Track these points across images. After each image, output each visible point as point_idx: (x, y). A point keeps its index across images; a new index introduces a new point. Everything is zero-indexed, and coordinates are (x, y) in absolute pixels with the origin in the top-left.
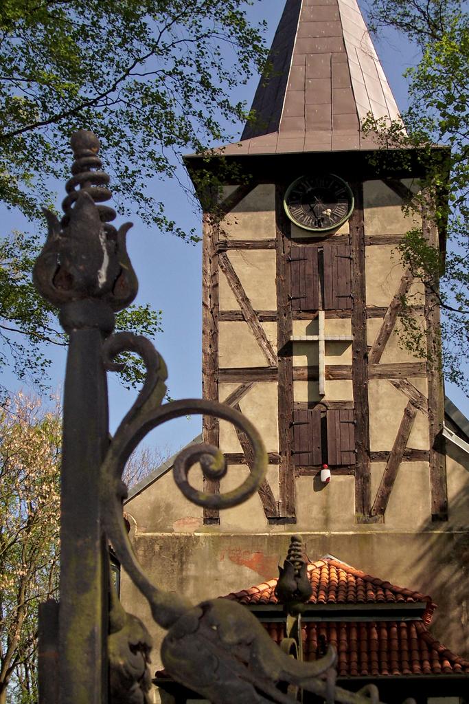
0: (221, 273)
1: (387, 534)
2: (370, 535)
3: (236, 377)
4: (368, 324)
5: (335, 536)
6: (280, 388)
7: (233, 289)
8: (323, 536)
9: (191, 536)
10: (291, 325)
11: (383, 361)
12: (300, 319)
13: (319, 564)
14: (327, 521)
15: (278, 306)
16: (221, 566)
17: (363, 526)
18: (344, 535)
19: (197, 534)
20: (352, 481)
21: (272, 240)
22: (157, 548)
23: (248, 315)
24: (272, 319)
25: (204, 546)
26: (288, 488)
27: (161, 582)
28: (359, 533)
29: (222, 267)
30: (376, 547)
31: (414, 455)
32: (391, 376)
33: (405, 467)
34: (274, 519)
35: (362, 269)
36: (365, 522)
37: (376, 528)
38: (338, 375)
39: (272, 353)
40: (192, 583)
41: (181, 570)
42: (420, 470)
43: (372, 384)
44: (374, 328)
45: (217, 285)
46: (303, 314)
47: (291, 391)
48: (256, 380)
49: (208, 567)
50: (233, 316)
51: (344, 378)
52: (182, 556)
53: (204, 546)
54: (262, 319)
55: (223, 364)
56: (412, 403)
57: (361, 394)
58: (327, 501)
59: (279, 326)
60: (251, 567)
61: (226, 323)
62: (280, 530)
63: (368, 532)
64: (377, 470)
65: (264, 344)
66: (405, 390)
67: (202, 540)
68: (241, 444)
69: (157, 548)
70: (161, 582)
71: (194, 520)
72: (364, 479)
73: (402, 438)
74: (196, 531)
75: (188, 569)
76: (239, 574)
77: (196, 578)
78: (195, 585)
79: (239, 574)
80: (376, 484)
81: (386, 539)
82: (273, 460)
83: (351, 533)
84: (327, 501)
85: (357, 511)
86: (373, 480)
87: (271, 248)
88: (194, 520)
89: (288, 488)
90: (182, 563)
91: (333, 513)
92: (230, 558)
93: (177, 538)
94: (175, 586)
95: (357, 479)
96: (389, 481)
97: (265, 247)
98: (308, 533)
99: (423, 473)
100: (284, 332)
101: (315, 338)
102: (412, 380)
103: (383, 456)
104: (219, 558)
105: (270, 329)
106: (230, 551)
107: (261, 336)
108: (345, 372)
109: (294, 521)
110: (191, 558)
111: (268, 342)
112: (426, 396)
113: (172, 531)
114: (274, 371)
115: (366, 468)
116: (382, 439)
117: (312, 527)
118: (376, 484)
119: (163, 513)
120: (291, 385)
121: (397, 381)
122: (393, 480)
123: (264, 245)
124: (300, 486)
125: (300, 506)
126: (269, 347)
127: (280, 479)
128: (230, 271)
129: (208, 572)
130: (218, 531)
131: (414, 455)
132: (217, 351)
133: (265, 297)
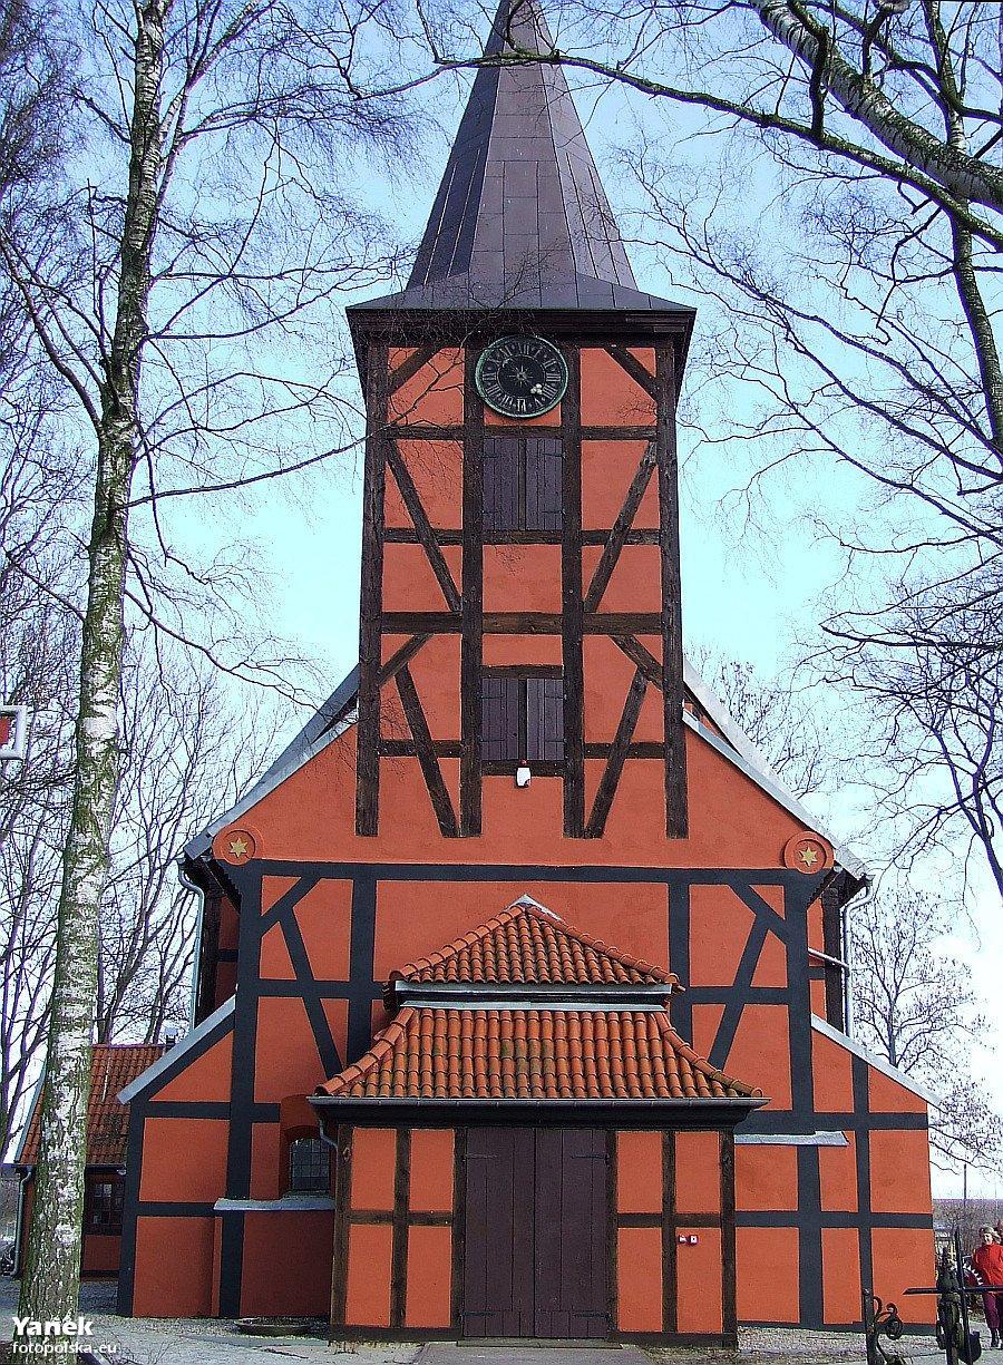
23: (425, 535)
26: (471, 793)
31: (647, 750)
50: (401, 535)
55: (388, 606)
64: (594, 770)
72: (575, 781)
73: (628, 724)
82: (451, 749)
89: (471, 793)
96: (609, 787)
103: (599, 750)
105: (454, 555)
116: (601, 726)
123: (447, 434)
131: (647, 750)
133: (447, 513)
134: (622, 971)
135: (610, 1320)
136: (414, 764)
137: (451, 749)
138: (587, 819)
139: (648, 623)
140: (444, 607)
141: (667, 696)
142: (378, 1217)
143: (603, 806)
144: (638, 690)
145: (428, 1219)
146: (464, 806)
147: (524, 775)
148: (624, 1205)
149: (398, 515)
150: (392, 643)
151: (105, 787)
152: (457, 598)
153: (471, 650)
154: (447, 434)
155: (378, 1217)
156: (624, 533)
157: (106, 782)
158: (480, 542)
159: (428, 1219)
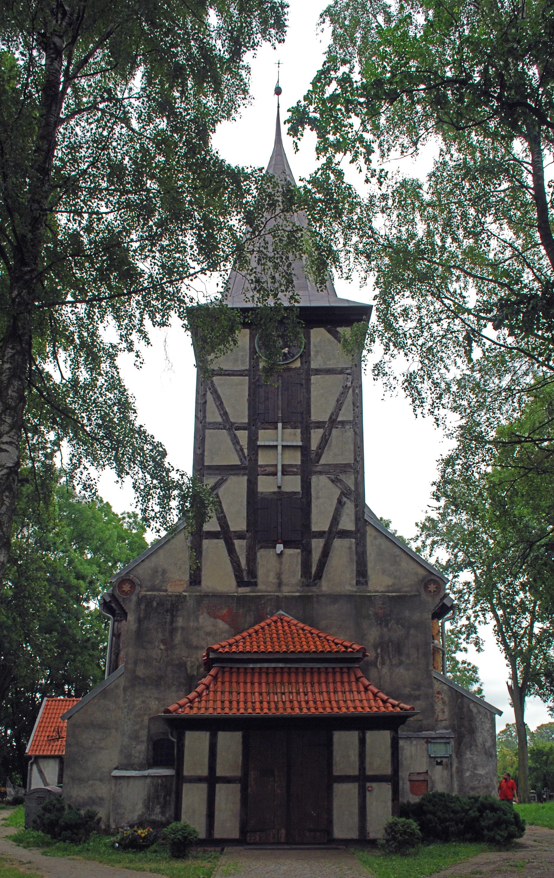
0: (209, 393)
1: (323, 596)
2: (311, 596)
3: (217, 472)
4: (312, 434)
5: (286, 596)
6: (249, 481)
7: (217, 406)
8: (278, 596)
9: (180, 595)
10: (257, 434)
11: (322, 462)
12: (265, 429)
13: (274, 618)
15: (249, 419)
16: (201, 620)
17: (306, 588)
18: (293, 596)
19: (184, 594)
20: (298, 553)
21: (246, 370)
22: (155, 604)
24: (244, 429)
25: (190, 603)
27: (157, 632)
28: (303, 594)
29: (210, 389)
30: (315, 606)
31: (344, 534)
32: (327, 473)
33: (337, 543)
34: (241, 583)
35: (309, 391)
36: (308, 586)
37: (315, 590)
38: (291, 471)
39: (244, 454)
40: (180, 632)
41: (172, 622)
42: (348, 545)
43: (314, 479)
44: (316, 436)
45: (205, 403)
46: (267, 425)
47: (256, 484)
48: (231, 475)
49: (192, 619)
50: (216, 426)
51: (295, 474)
52: (173, 610)
53: (190, 603)
54: (238, 429)
56: (342, 494)
57: (306, 485)
58: (280, 569)
59: (249, 434)
60: (223, 620)
61: (211, 431)
62: (244, 590)
63: (310, 594)
64: (317, 545)
65: (238, 448)
66: (338, 484)
67: (188, 598)
68: (219, 523)
69: (155, 604)
70: (157, 632)
71: (182, 583)
72: (307, 551)
73: (335, 520)
74: (184, 591)
75: (177, 620)
76: (214, 626)
77: (183, 629)
79: (214, 626)
80: (316, 556)
83: (298, 594)
84: (280, 569)
85: (302, 576)
86: (313, 552)
87: (245, 376)
88: (182, 583)
89: (252, 559)
90: (173, 616)
91: (284, 578)
92: (209, 613)
93: (170, 596)
94: (167, 634)
95: (302, 552)
96: (326, 553)
97: (241, 375)
98: (266, 594)
99: (350, 548)
100: (253, 440)
101: (275, 443)
102: (342, 477)
103: (320, 534)
105: (243, 436)
107: (235, 441)
108: (295, 470)
109: (256, 584)
110: (179, 613)
111: (241, 446)
112: (353, 488)
113: (166, 591)
114: (245, 468)
115: (309, 544)
117: (269, 589)
118: (316, 556)
119: (160, 577)
120: (256, 479)
121: (333, 477)
122: (329, 553)
123: (240, 373)
124: (261, 557)
125: (261, 572)
126: (242, 450)
127: (247, 551)
128: (215, 392)
129: (192, 624)
130: (200, 591)
131: (344, 534)
132: (204, 451)
134: (334, 647)
135: (329, 831)
136: (221, 543)
137: (240, 536)
138: (313, 573)
139: (344, 468)
140: (236, 461)
141: (356, 506)
142: (199, 780)
143: (322, 564)
144: (340, 503)
145: (227, 780)
146: (248, 564)
147: (280, 547)
148: (337, 772)
149: (214, 416)
150: (210, 481)
151: (7, 497)
152: (245, 457)
153: (252, 485)
154: (240, 373)
155: (199, 780)
156: (333, 422)
157: (7, 494)
158: (257, 429)
159: (227, 780)
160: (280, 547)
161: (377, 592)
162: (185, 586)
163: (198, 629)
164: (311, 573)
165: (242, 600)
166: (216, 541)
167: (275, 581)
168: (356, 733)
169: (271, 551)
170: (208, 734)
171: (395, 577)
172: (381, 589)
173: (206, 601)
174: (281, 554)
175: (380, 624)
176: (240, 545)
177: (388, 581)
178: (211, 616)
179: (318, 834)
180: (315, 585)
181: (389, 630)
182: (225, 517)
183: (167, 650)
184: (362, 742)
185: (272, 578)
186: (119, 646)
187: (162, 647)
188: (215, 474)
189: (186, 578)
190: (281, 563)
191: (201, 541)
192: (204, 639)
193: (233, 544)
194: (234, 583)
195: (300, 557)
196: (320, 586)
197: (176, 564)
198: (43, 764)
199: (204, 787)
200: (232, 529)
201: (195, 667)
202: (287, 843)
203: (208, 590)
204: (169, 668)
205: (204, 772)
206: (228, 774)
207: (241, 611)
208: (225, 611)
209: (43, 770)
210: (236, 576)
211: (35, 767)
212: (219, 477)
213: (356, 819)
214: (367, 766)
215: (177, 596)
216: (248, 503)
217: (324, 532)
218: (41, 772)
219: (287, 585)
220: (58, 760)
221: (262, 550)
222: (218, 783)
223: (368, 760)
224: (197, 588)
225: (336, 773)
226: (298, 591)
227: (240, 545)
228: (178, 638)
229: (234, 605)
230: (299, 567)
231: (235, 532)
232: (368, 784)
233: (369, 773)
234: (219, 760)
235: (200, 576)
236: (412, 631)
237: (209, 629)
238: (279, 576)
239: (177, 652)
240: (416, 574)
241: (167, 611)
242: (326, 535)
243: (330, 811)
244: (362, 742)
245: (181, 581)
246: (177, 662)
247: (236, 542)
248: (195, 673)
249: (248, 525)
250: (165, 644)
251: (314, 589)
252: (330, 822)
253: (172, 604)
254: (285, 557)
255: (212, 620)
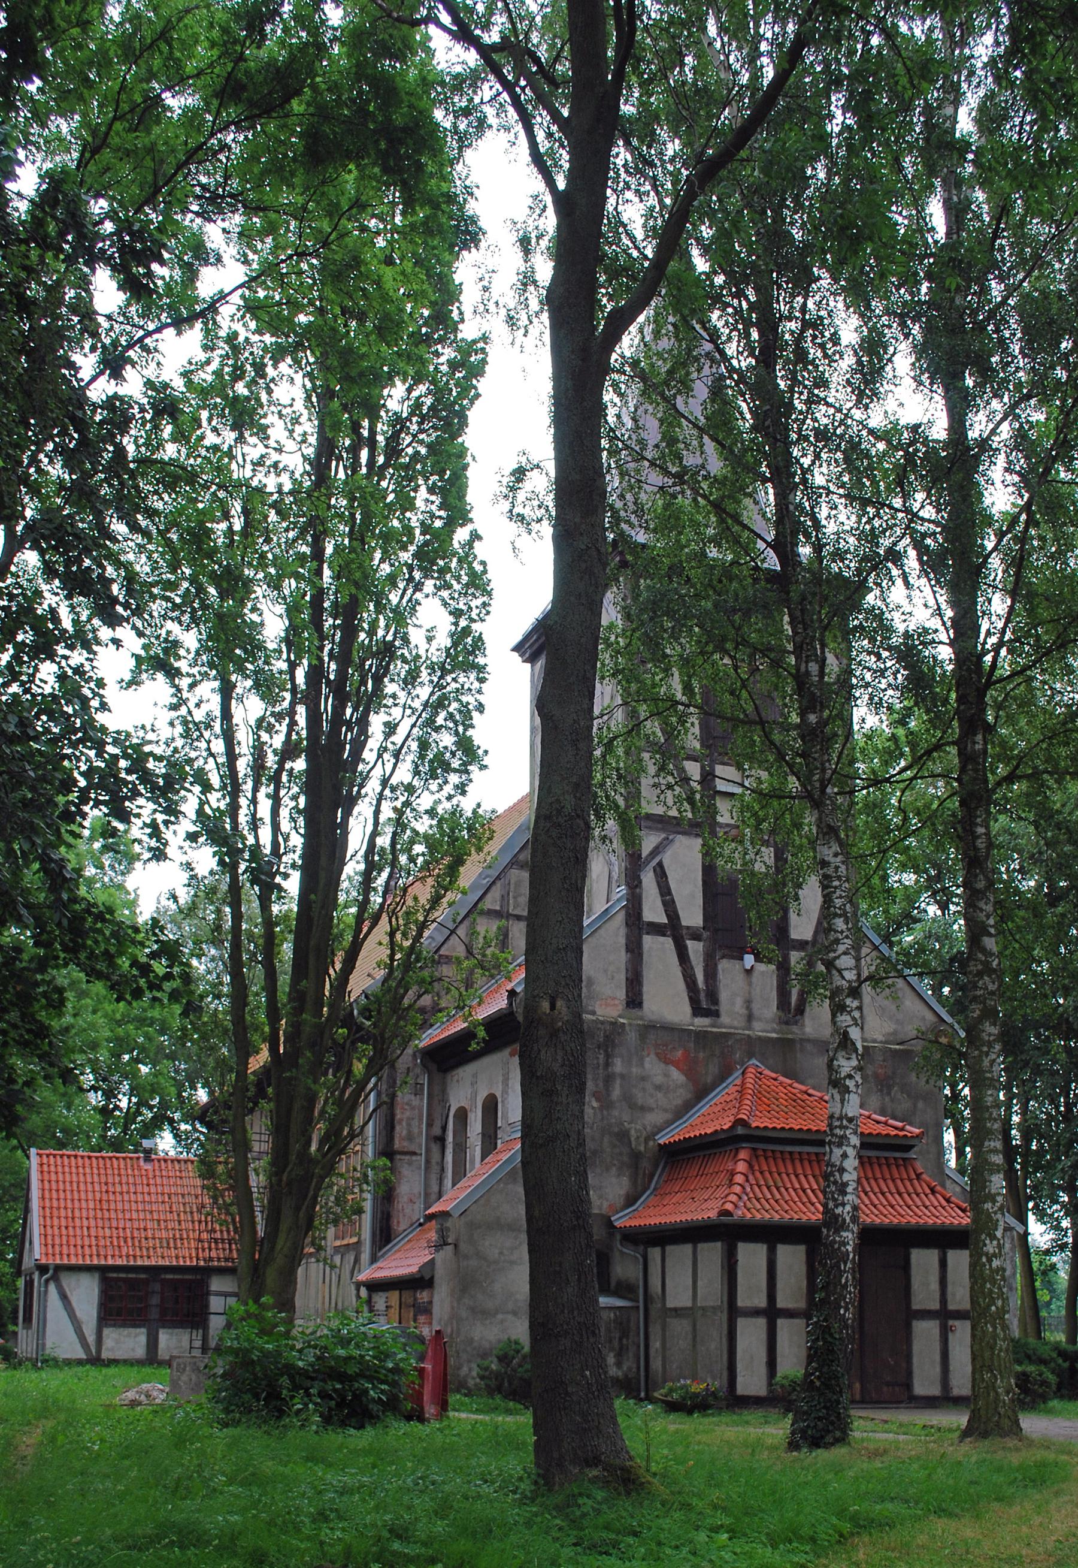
1: (809, 1040)
2: (791, 1042)
5: (760, 1038)
14: (750, 1017)
16: (647, 1065)
17: (784, 1027)
25: (632, 1036)
26: (711, 974)
34: (697, 1010)
36: (787, 1023)
40: (618, 1081)
41: (607, 1064)
53: (632, 1036)
60: (678, 1068)
67: (627, 1028)
77: (623, 1076)
78: (621, 1086)
79: (666, 1075)
81: (809, 1047)
83: (774, 1035)
89: (711, 974)
90: (608, 1056)
91: (756, 1007)
92: (657, 1054)
93: (602, 1023)
94: (601, 1085)
95: (778, 969)
104: (645, 1053)
106: (657, 1046)
109: (716, 1014)
110: (617, 1051)
113: (594, 1013)
117: (736, 1023)
125: (724, 996)
129: (634, 1070)
130: (641, 1018)
135: (908, 1386)
142: (756, 1313)
145: (790, 1314)
147: (749, 960)
155: (756, 1313)
159: (790, 1314)
160: (749, 960)
161: (875, 1041)
162: (620, 1007)
163: (643, 1079)
164: (790, 1004)
165: (701, 1038)
166: (662, 939)
167: (744, 1011)
168: (936, 1251)
169: (737, 964)
170: (765, 1247)
171: (897, 1022)
172: (880, 1038)
173: (652, 1037)
174: (749, 972)
175: (881, 1091)
176: (695, 949)
177: (889, 1027)
178: (660, 1059)
179: (897, 1389)
180: (796, 1023)
181: (892, 1100)
182: (673, 901)
183: (601, 1108)
184: (943, 1264)
185: (739, 1006)
186: (395, 1082)
187: (595, 1104)
188: (658, 830)
189: (622, 994)
190: (750, 984)
191: (641, 938)
192: (651, 1096)
193: (686, 947)
194: (688, 1009)
195: (775, 977)
196: (803, 1025)
197: (606, 971)
198: (68, 1281)
199: (762, 1322)
200: (684, 923)
201: (642, 1140)
202: (862, 1402)
203: (654, 1018)
204: (606, 1140)
205: (762, 1302)
206: (791, 1305)
207: (701, 1055)
208: (679, 1053)
209: (68, 1293)
210: (690, 998)
211: (52, 1287)
212: (663, 836)
213: (938, 1369)
214: (949, 1298)
215: (612, 1023)
216: (705, 883)
217: (807, 942)
218: (64, 1297)
219: (760, 1020)
220: (97, 1275)
221: (725, 961)
222: (779, 1317)
223: (950, 1288)
224: (635, 1012)
225: (915, 1306)
226: (774, 1031)
227: (695, 949)
228: (616, 1093)
229: (692, 1045)
230: (775, 993)
231: (688, 928)
232: (951, 1322)
233: (951, 1307)
234: (780, 1285)
235: (640, 994)
236: (920, 1105)
237: (659, 1079)
238: (748, 1003)
239: (616, 1113)
240: (924, 1019)
241: (599, 1048)
242: (809, 947)
243: (908, 1357)
244: (943, 1264)
245: (614, 999)
246: (616, 1130)
247: (689, 943)
248: (642, 1148)
249: (705, 920)
250: (598, 1100)
251: (795, 1029)
252: (909, 1374)
253: (606, 1037)
254: (755, 974)
255: (662, 1065)
